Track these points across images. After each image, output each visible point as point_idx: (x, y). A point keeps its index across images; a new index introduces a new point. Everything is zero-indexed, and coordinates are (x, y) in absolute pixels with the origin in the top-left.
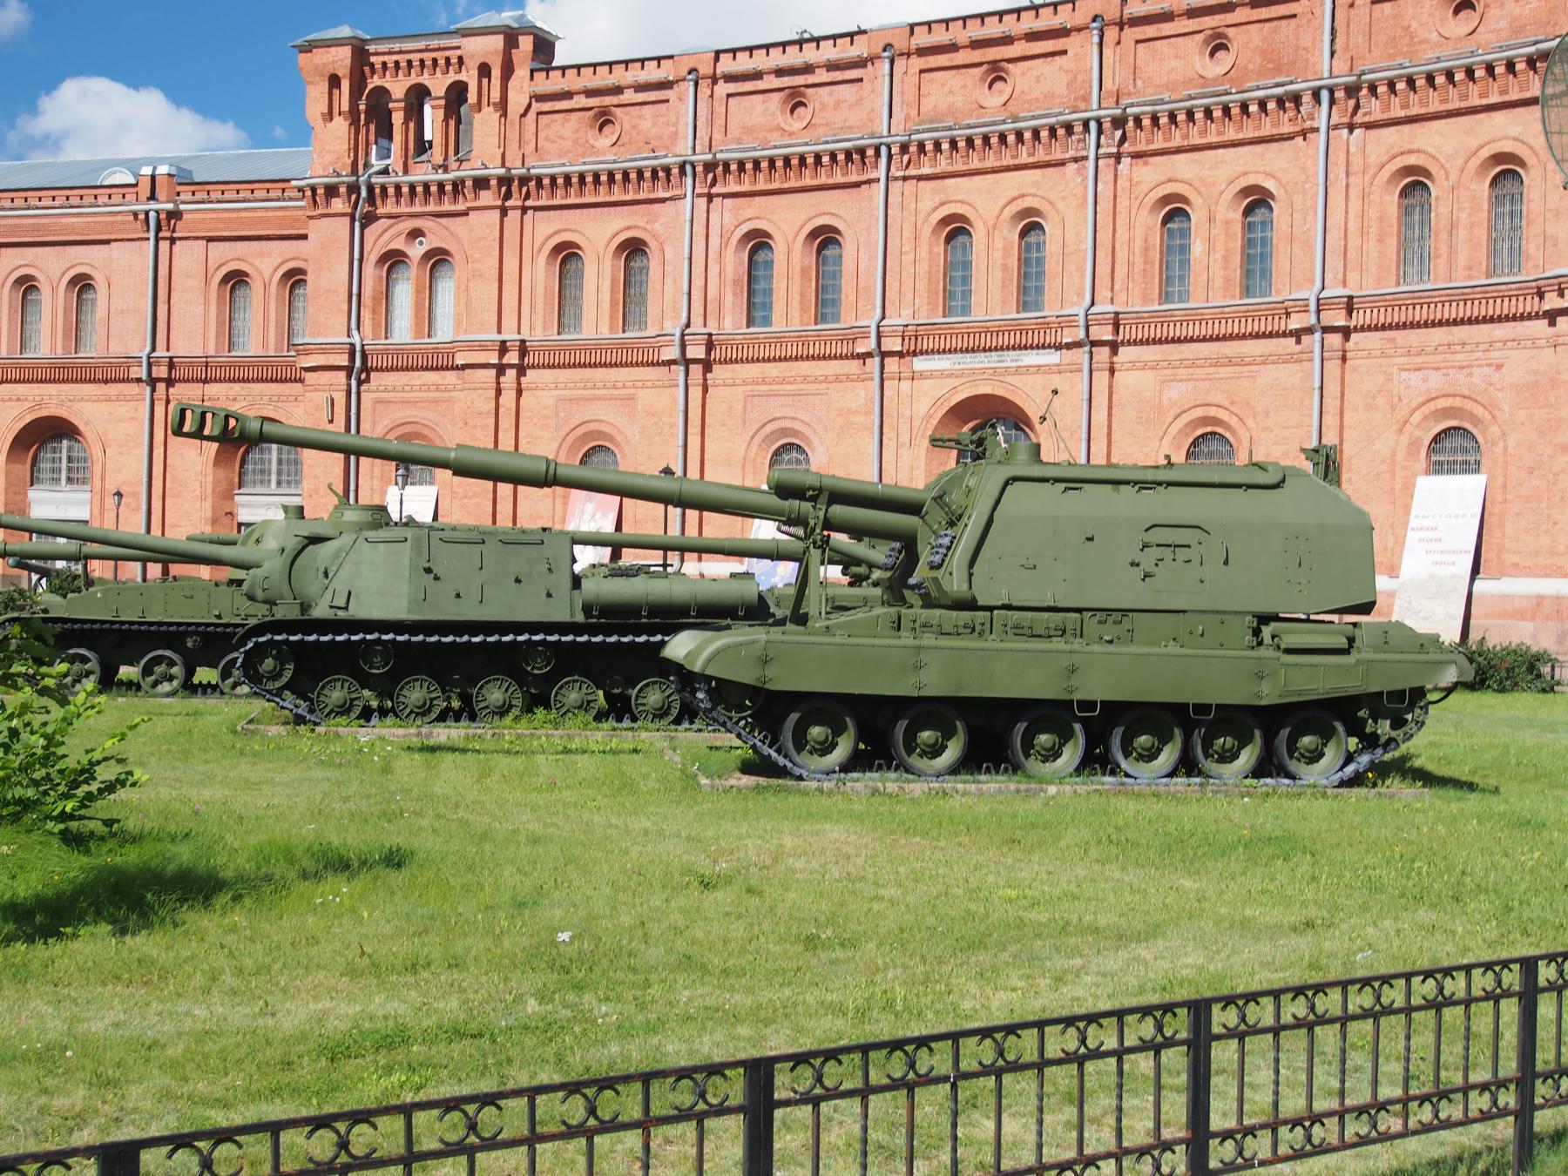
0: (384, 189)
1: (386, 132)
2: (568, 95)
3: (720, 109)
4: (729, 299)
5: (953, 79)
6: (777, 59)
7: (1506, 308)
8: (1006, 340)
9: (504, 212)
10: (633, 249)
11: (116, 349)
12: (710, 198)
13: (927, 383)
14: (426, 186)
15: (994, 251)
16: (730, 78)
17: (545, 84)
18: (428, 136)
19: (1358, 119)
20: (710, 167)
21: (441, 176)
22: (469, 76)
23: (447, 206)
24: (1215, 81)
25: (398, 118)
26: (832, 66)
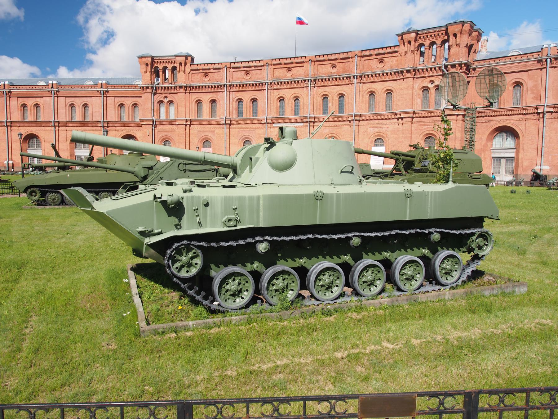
0: (159, 88)
2: (199, 70)
4: (234, 112)
5: (281, 70)
6: (244, 65)
7: (389, 117)
8: (292, 121)
9: (185, 93)
10: (213, 101)
11: (95, 120)
12: (230, 91)
14: (168, 87)
15: (289, 104)
16: (233, 68)
18: (167, 77)
19: (362, 81)
20: (230, 85)
21: (171, 85)
23: (172, 92)
24: (334, 73)
25: (161, 73)
26: (255, 67)
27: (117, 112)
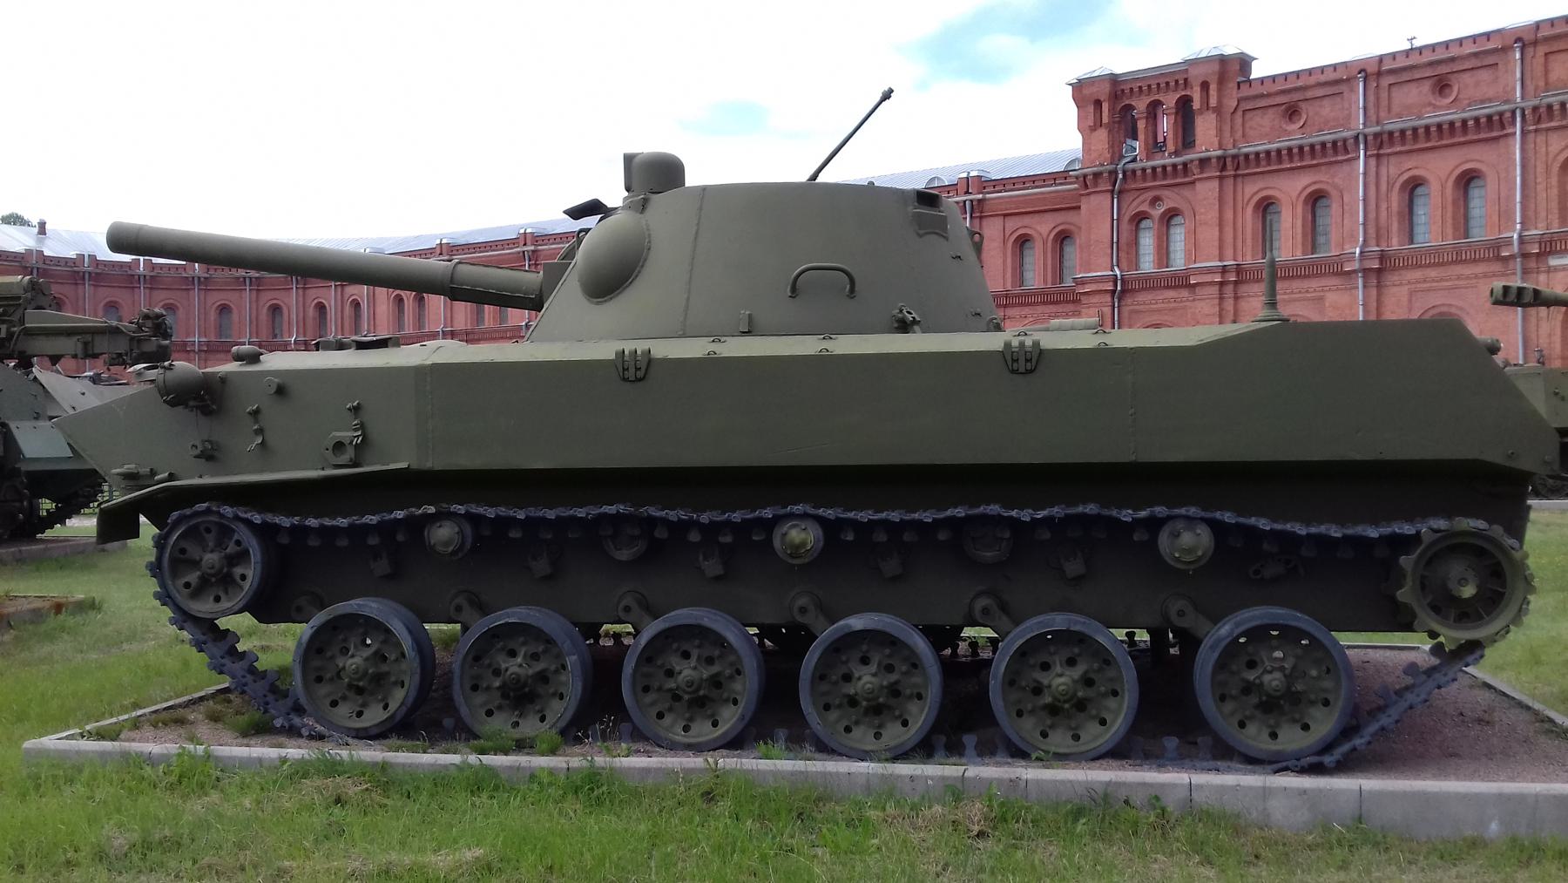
3: (1384, 95)
13: (1560, 275)
25: (1141, 125)
27: (1009, 260)
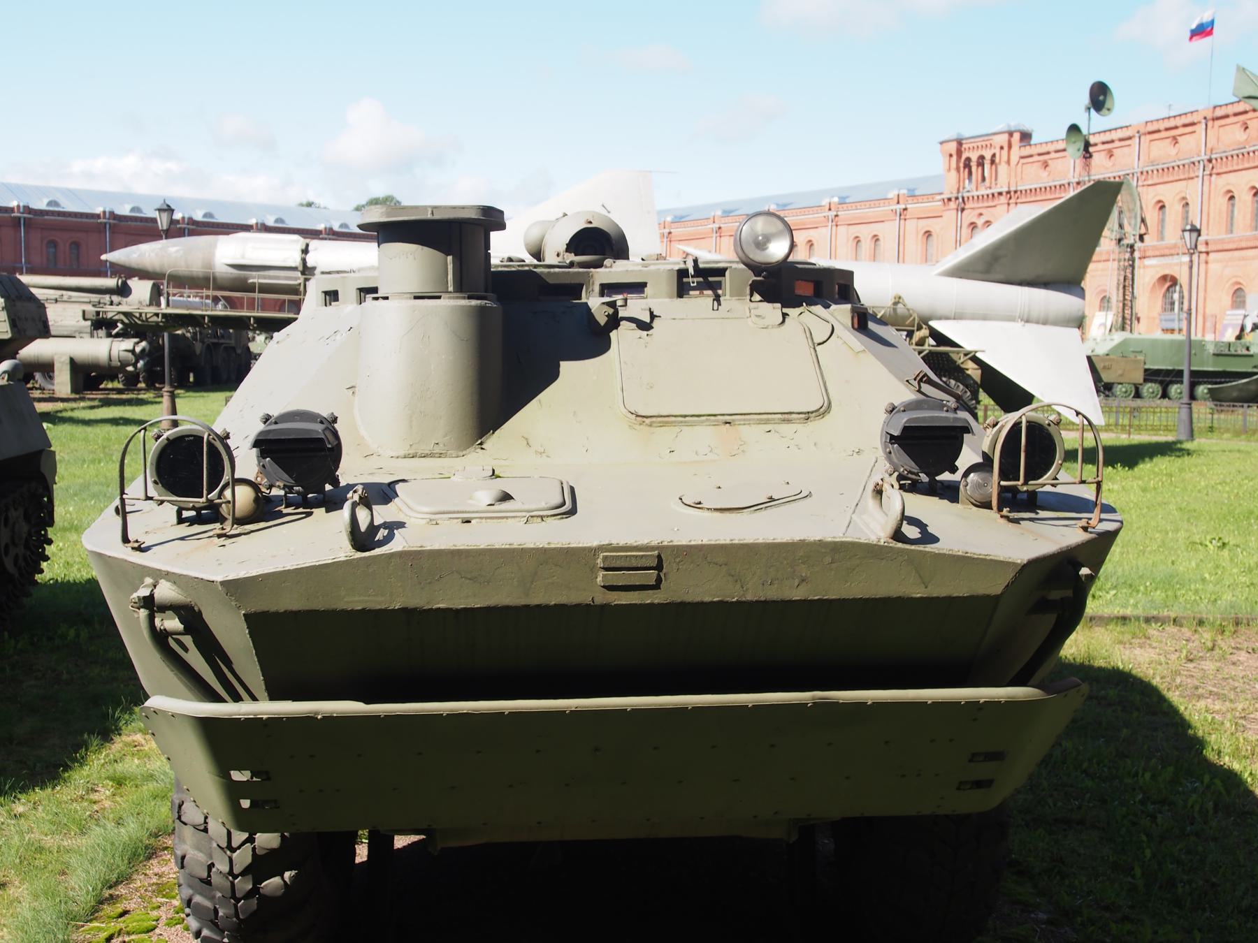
1: (970, 173)
17: (1027, 151)
21: (989, 192)
22: (997, 151)
23: (991, 204)
25: (974, 169)
26: (1121, 140)
